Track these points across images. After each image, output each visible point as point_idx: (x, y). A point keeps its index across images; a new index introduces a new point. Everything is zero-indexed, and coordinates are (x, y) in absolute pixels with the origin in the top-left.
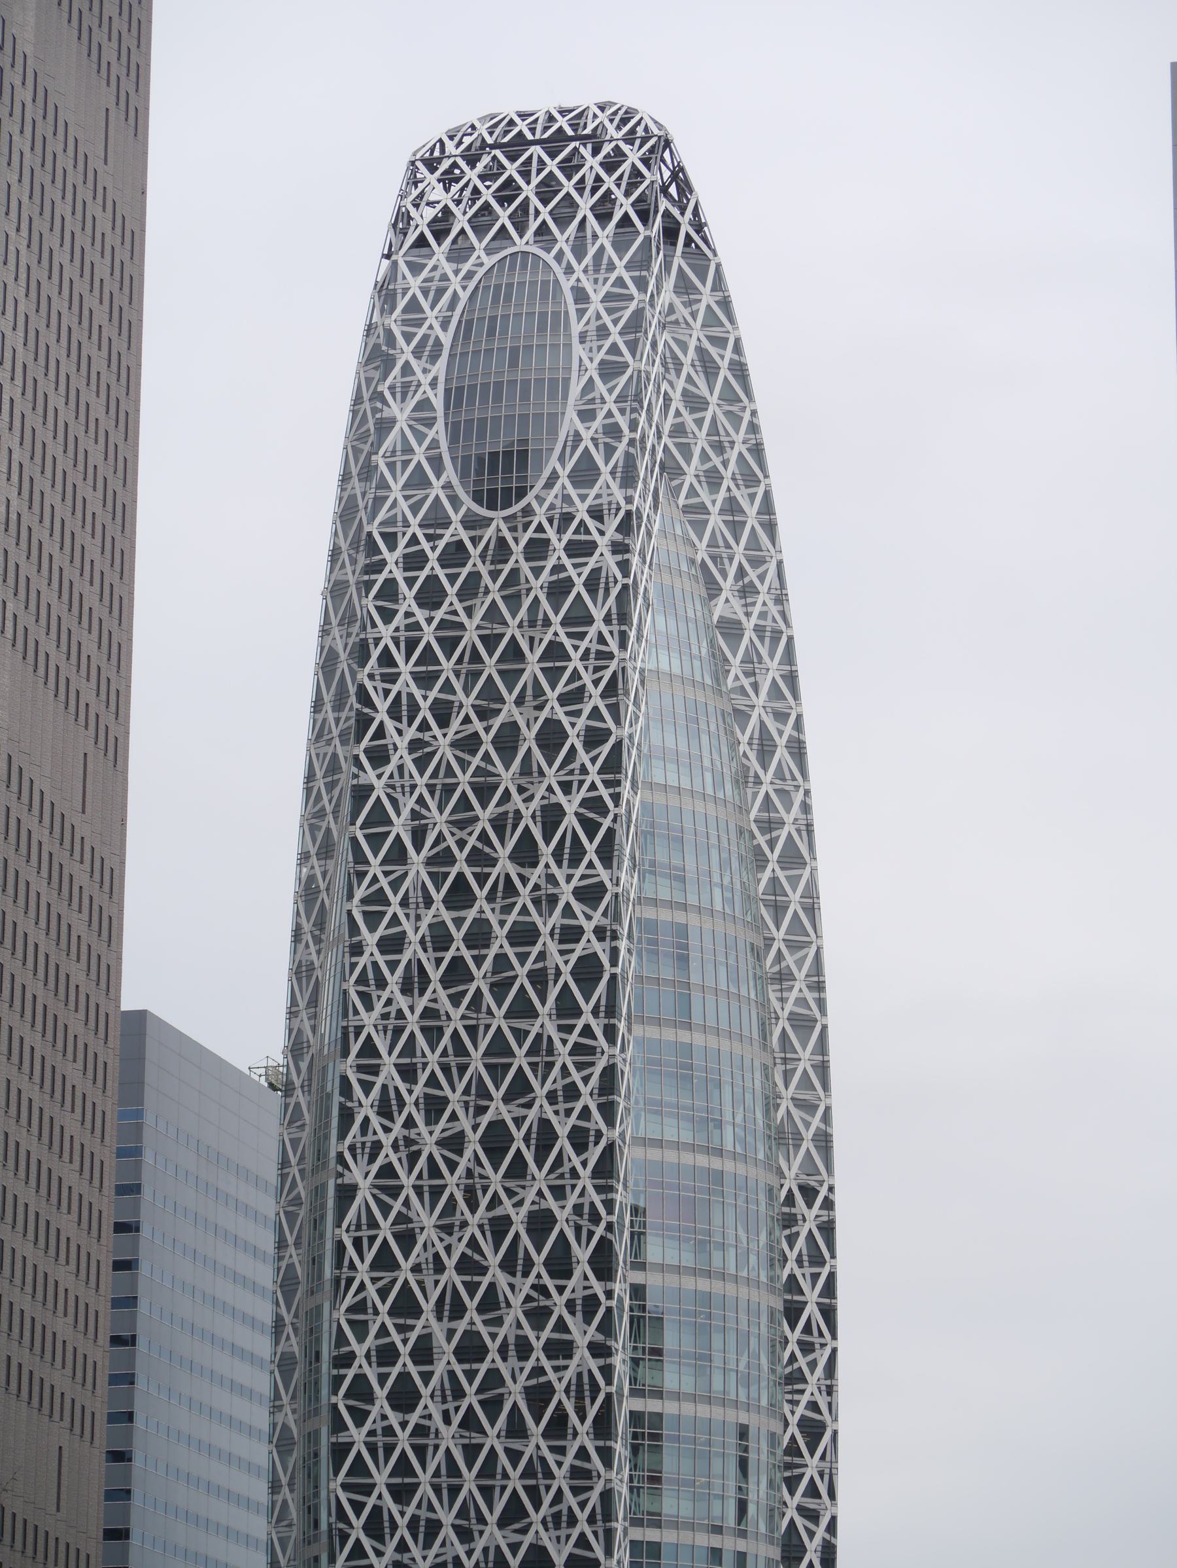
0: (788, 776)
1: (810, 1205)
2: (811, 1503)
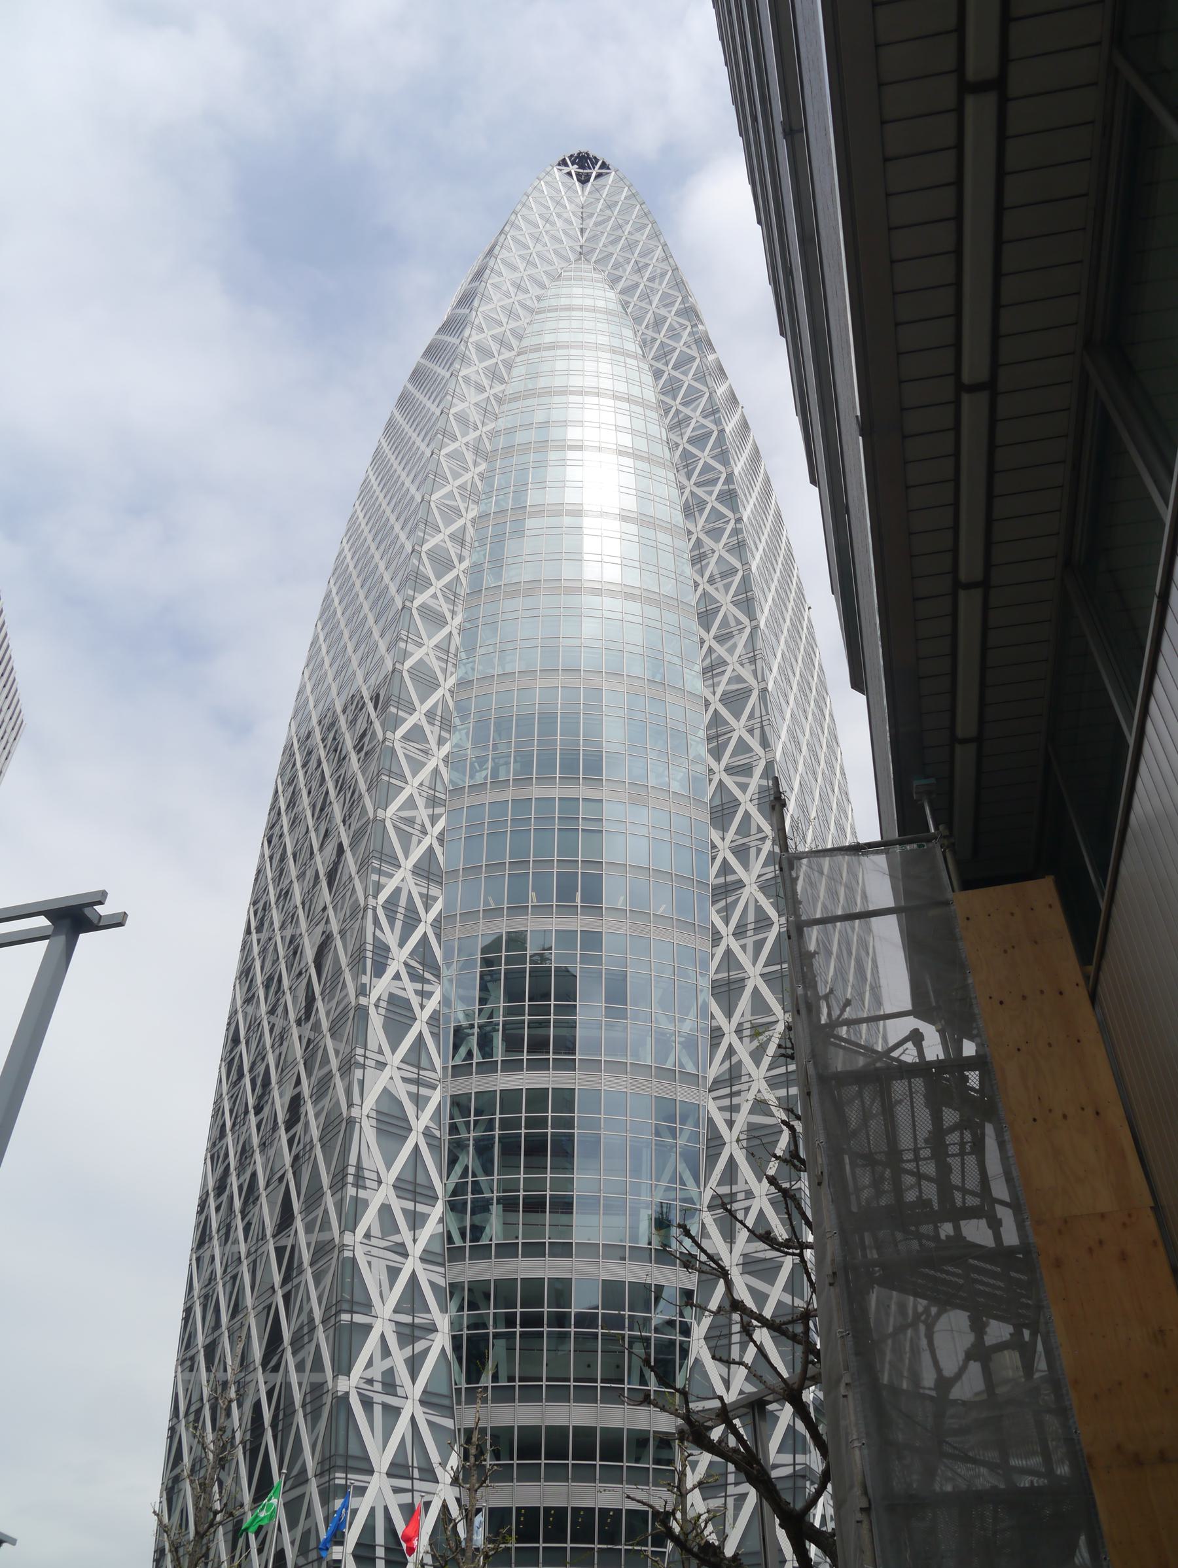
0: (677, 326)
1: (717, 541)
2: (742, 760)
